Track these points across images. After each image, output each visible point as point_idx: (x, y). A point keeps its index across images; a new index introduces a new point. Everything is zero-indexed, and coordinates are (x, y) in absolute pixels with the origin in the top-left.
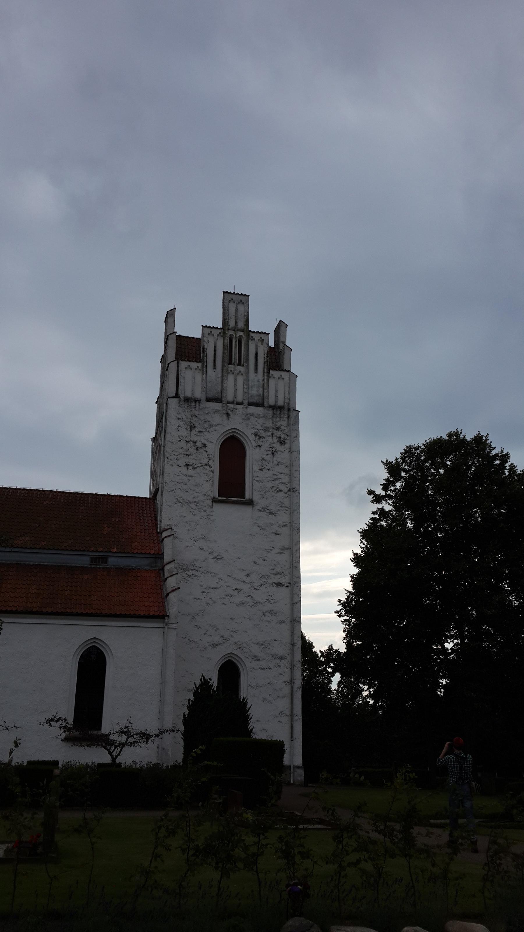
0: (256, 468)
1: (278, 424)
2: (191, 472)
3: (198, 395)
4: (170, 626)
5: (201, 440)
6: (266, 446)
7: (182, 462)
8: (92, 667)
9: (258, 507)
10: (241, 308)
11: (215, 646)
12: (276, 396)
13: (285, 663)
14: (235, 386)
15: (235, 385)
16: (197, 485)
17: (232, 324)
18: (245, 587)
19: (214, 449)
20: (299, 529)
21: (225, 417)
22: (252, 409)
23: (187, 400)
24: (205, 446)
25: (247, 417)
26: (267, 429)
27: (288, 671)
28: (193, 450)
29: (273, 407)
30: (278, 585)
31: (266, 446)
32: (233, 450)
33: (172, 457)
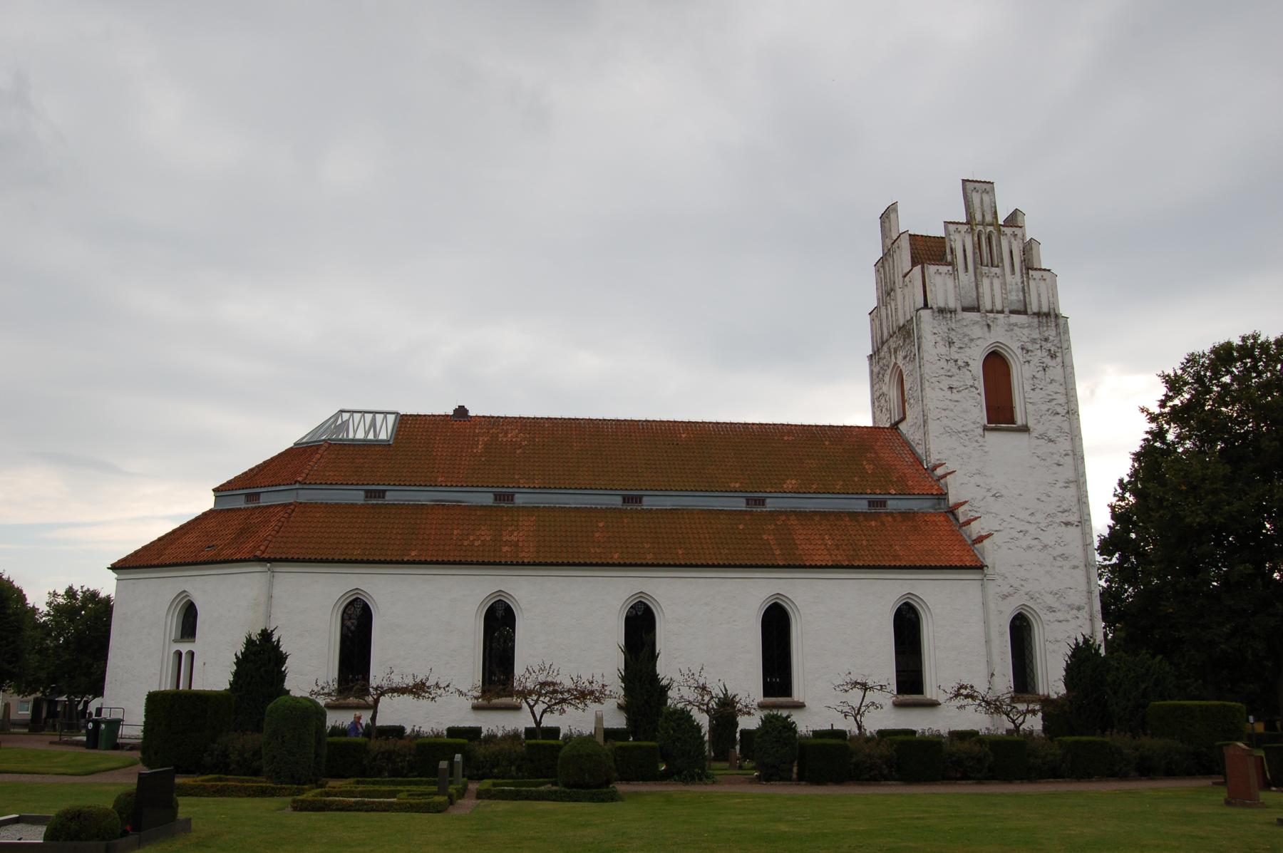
0: (1027, 388)
1: (1046, 334)
2: (956, 396)
3: (952, 305)
4: (988, 577)
5: (962, 358)
6: (1035, 361)
7: (945, 385)
8: (907, 625)
9: (1035, 434)
10: (986, 198)
11: (1005, 597)
12: (1040, 301)
13: (1084, 614)
14: (994, 290)
15: (992, 290)
16: (965, 411)
17: (978, 217)
18: (1031, 528)
19: (977, 367)
20: (1083, 458)
21: (986, 328)
22: (1015, 318)
23: (941, 311)
24: (967, 364)
25: (1011, 328)
26: (1034, 341)
27: (1088, 623)
28: (955, 370)
29: (1038, 314)
30: (1067, 524)
31: (1035, 361)
32: (996, 366)
33: (934, 380)
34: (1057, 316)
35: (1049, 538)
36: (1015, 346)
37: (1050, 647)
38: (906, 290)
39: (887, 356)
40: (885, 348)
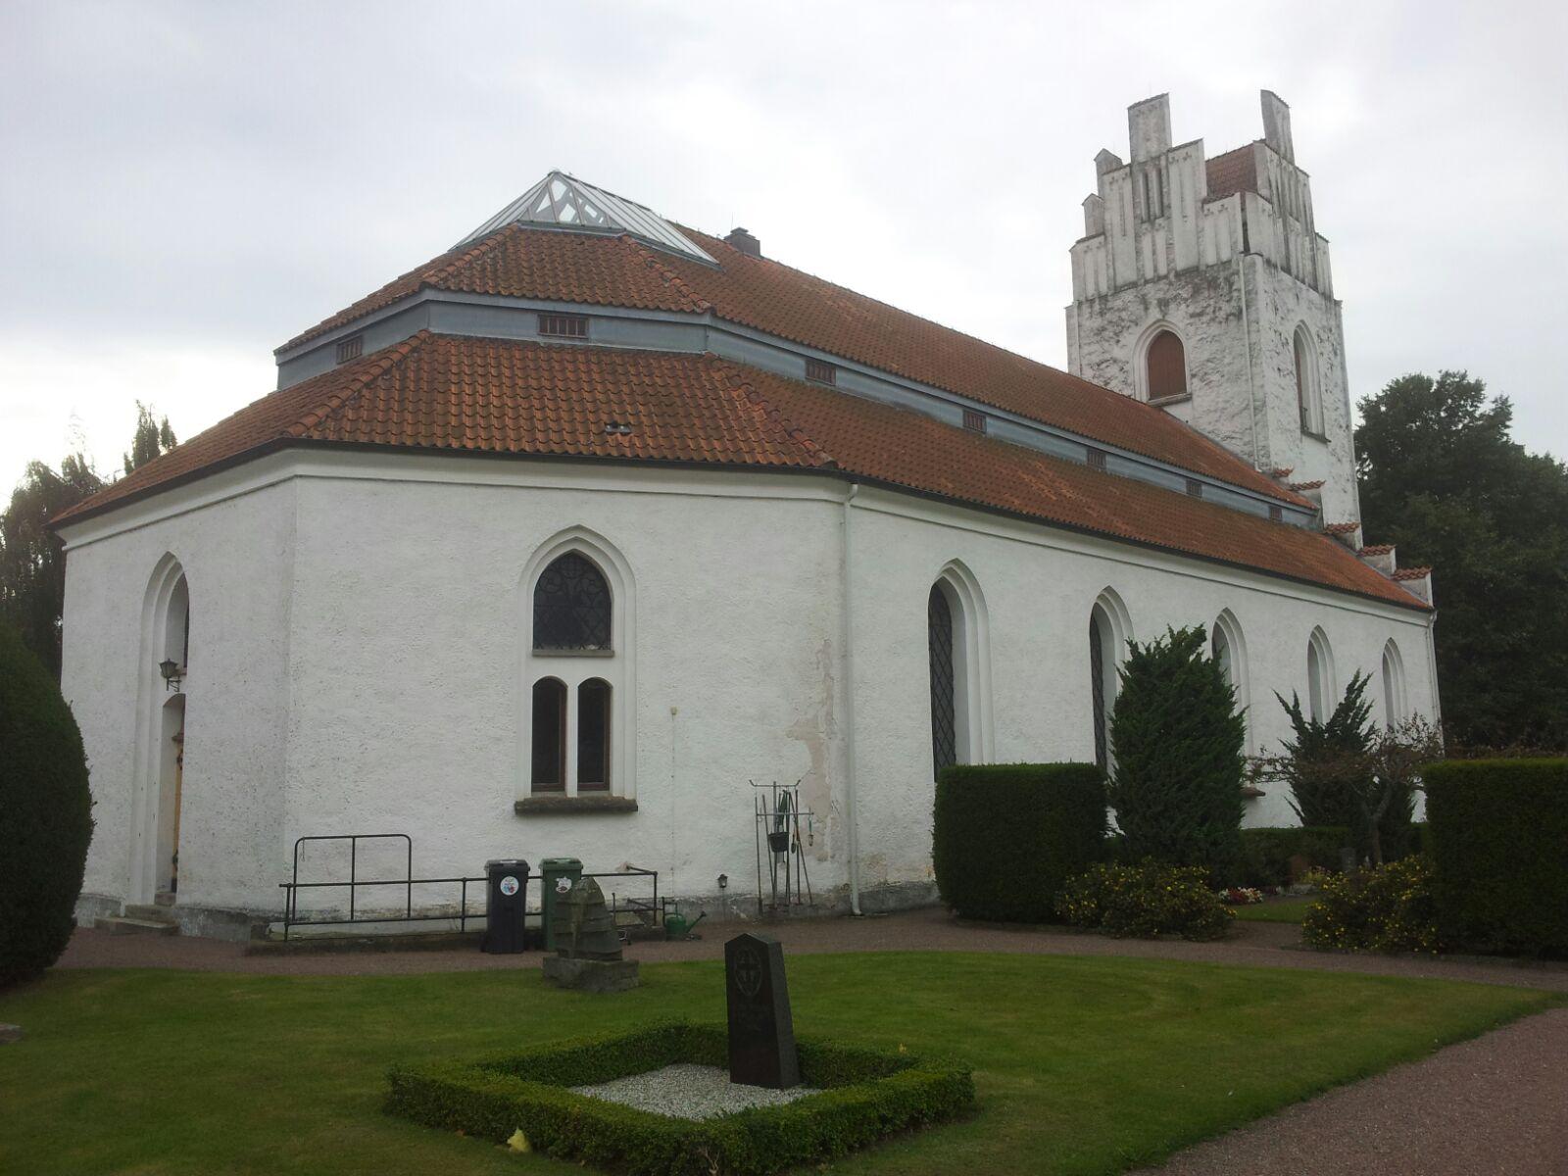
9: (1331, 446)
34: (1338, 303)
36: (1313, 330)
38: (1208, 224)
39: (1136, 309)
40: (1129, 296)
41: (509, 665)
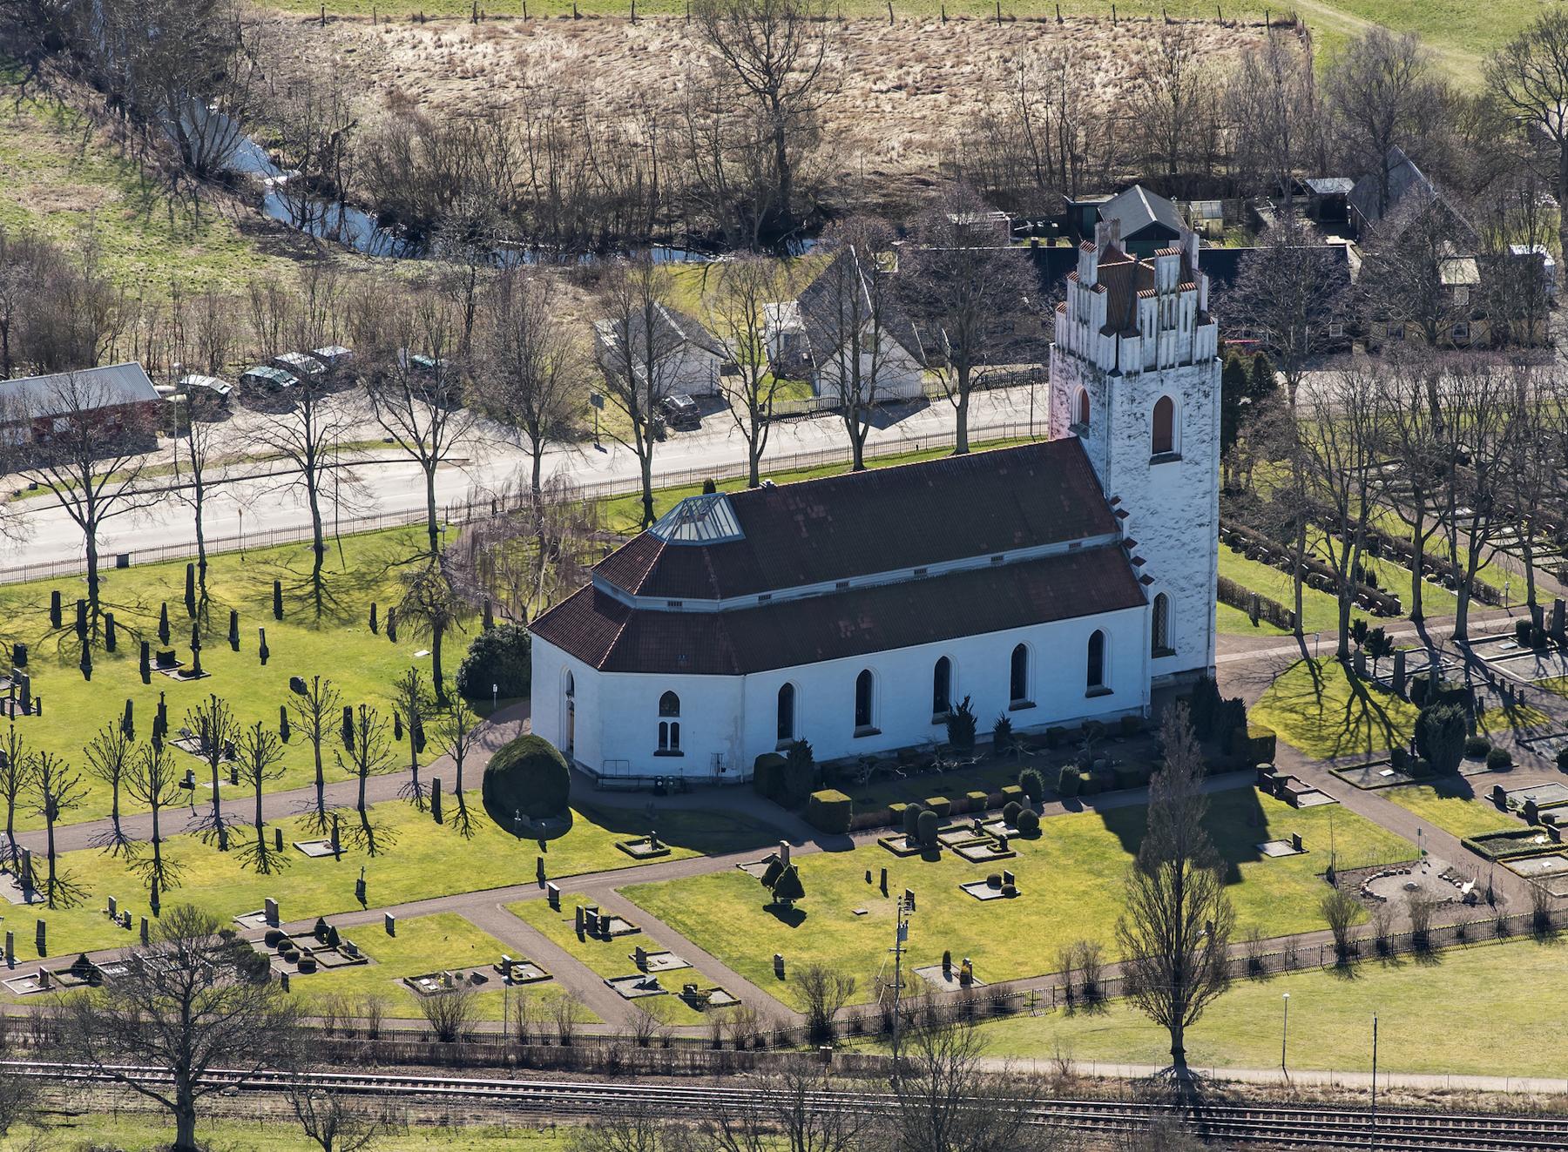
2: (1133, 442)
7: (1125, 435)
18: (1174, 533)
23: (1129, 374)
26: (1194, 386)
29: (1199, 362)
31: (1193, 402)
35: (1185, 538)
37: (1179, 616)
41: (653, 719)
